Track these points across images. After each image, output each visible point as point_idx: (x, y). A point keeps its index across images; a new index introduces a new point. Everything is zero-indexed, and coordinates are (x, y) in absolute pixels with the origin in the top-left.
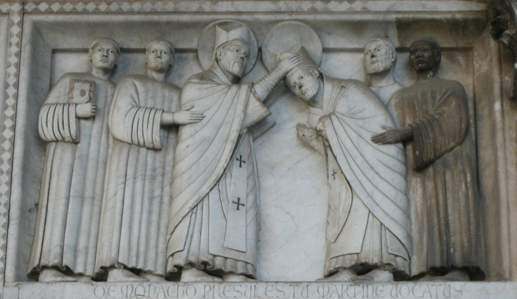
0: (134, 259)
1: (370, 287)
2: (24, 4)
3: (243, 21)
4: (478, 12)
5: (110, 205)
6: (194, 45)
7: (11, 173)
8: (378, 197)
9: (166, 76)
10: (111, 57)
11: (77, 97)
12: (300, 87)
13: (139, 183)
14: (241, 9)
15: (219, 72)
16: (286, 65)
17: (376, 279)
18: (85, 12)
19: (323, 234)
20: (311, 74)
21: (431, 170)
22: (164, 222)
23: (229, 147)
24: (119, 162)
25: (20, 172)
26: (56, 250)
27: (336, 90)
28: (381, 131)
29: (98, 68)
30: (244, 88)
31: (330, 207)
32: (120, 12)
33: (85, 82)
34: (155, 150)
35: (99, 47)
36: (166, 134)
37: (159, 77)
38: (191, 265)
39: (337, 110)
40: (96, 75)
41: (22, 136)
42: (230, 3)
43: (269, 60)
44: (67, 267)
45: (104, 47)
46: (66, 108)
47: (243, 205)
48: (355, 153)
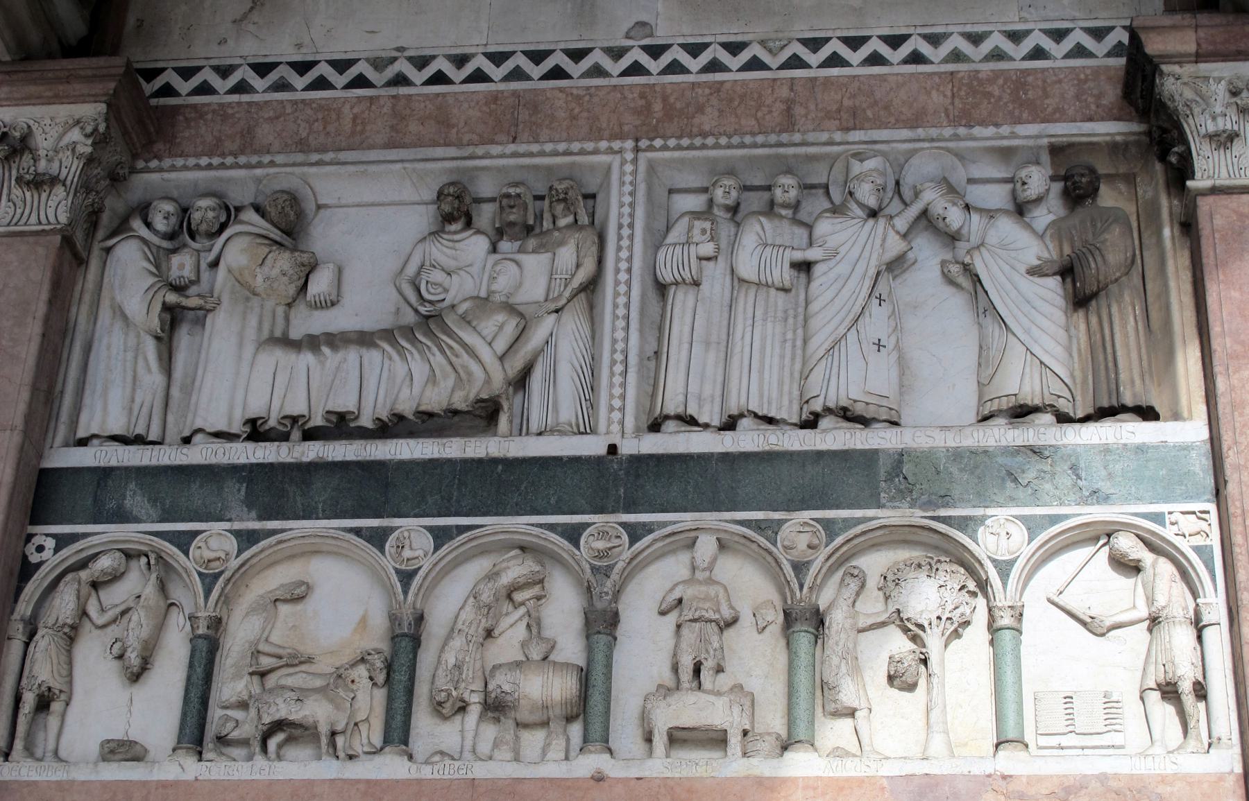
0: (765, 406)
1: (1031, 430)
2: (637, 140)
4: (1140, 133)
5: (737, 349)
7: (627, 317)
8: (1036, 332)
9: (794, 213)
10: (734, 194)
11: (697, 236)
12: (944, 219)
13: (769, 325)
15: (854, 206)
17: (1037, 422)
18: (704, 147)
19: (975, 377)
20: (955, 204)
21: (1094, 303)
22: (798, 366)
23: (868, 283)
24: (745, 303)
27: (985, 220)
28: (1037, 262)
30: (882, 222)
31: (981, 347)
32: (742, 146)
33: (706, 219)
34: (786, 290)
35: (720, 183)
36: (796, 274)
38: (828, 411)
39: (986, 241)
40: (718, 213)
41: (639, 279)
42: (862, 132)
43: (907, 193)
44: (692, 417)
45: (726, 182)
46: (686, 248)
47: (885, 347)
48: (1009, 286)
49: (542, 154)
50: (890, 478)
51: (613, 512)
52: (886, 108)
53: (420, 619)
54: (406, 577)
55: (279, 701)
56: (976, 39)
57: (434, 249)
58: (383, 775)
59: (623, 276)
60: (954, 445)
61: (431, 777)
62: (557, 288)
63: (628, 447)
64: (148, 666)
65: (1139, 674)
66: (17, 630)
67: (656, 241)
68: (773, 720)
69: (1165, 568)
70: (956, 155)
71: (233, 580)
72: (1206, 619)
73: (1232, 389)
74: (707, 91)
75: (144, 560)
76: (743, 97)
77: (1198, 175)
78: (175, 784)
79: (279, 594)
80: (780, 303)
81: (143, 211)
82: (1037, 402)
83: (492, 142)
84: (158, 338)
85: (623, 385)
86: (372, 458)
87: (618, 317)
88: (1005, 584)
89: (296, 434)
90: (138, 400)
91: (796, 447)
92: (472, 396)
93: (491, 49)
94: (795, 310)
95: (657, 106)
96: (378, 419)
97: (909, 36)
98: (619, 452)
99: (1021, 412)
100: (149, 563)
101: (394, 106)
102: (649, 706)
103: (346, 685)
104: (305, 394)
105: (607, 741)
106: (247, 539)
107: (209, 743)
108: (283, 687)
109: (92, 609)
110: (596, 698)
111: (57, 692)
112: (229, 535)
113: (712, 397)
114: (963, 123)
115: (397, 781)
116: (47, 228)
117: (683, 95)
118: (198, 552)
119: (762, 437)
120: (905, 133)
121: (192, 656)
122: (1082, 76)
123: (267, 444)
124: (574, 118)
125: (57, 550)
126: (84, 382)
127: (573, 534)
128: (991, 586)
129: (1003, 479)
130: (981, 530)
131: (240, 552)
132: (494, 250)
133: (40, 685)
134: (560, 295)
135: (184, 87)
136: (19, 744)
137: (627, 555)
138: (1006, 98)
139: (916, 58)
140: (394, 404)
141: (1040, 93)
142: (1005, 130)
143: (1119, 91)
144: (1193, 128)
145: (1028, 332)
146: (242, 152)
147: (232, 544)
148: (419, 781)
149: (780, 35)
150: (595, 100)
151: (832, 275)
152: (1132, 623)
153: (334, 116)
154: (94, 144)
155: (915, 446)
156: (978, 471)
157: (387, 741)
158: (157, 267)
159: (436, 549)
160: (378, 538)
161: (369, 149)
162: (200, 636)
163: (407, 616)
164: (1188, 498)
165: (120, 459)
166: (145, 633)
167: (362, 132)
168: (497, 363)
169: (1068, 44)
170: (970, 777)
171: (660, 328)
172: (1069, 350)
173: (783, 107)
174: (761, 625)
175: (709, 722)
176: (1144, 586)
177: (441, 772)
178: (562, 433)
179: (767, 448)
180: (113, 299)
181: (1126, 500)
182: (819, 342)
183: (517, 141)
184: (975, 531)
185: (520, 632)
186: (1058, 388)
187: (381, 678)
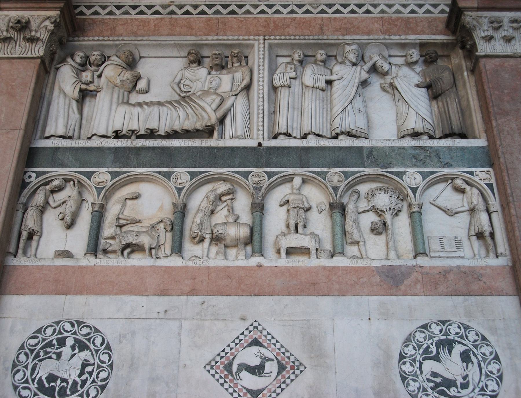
0: (318, 130)
2: (264, 36)
3: (356, 43)
4: (453, 40)
5: (306, 110)
6: (335, 54)
7: (263, 98)
13: (318, 102)
14: (355, 38)
15: (347, 62)
16: (376, 58)
18: (290, 39)
19: (395, 124)
20: (386, 62)
21: (440, 98)
22: (329, 118)
23: (355, 88)
24: (308, 94)
25: (267, 98)
26: (285, 127)
27: (397, 68)
29: (296, 60)
31: (397, 113)
33: (292, 64)
34: (323, 90)
35: (297, 52)
37: (323, 64)
38: (343, 133)
43: (366, 59)
44: (290, 134)
46: (285, 74)
48: (408, 90)
49: (228, 40)
50: (368, 157)
51: (261, 167)
52: (358, 28)
53: (185, 206)
54: (179, 190)
55: (129, 236)
56: (390, 6)
57: (186, 73)
58: (172, 264)
59: (261, 83)
60: (392, 146)
61: (192, 265)
62: (235, 87)
63: (266, 144)
64: (74, 223)
65: (467, 230)
66: (20, 208)
67: (272, 71)
68: (328, 246)
69: (475, 191)
70: (385, 45)
71: (109, 190)
72: (492, 209)
73: (498, 125)
74: (290, 20)
75: (72, 183)
76: (304, 23)
77: (479, 51)
78: (86, 267)
79: (127, 197)
80: (321, 95)
81: (72, 56)
82: (422, 131)
83: (208, 35)
84: (77, 101)
85: (263, 122)
86: (165, 146)
87: (260, 98)
88: (415, 196)
89: (133, 137)
90: (70, 123)
91: (331, 145)
92: (204, 125)
93: (207, 3)
94: (327, 98)
95: (272, 25)
96: (166, 132)
97: (365, 4)
98: (262, 145)
99: (416, 135)
100: (74, 184)
101: (170, 22)
102: (278, 239)
103: (156, 231)
104: (137, 122)
105: (262, 253)
106: (114, 175)
107: (100, 252)
108: (130, 231)
109: (51, 201)
110: (256, 236)
111: (36, 232)
112: (107, 173)
113: (297, 127)
114: (387, 34)
115: (178, 267)
116: (35, 56)
117: (281, 21)
118: (95, 180)
119: (318, 141)
120: (366, 37)
121: (92, 218)
122: (430, 20)
123: (122, 140)
124: (240, 28)
125: (37, 178)
126: (48, 117)
127: (246, 175)
128: (409, 196)
129: (411, 158)
130: (404, 176)
131: (111, 180)
132: (209, 73)
133: (29, 229)
134: (237, 90)
135: (88, 12)
136: (20, 251)
137: (267, 183)
138: (402, 26)
139: (368, 12)
140: (173, 126)
141: (415, 25)
142: (403, 37)
143: (444, 26)
144: (476, 35)
145: (417, 107)
146: (111, 36)
147: (109, 177)
148: (187, 267)
149: (317, 2)
150: (248, 22)
151: (341, 85)
152: (463, 212)
153: (147, 24)
154: (54, 26)
155: (376, 145)
156: (402, 155)
157: (173, 252)
158: (77, 75)
159: (191, 180)
160: (168, 175)
161: (161, 36)
162: (96, 211)
163: (180, 202)
164: (482, 166)
165: (63, 144)
166: (73, 209)
167: (158, 30)
168: (213, 112)
169: (424, 9)
170: (407, 267)
171: (274, 102)
172: (431, 113)
173: (319, 27)
174: (320, 210)
175: (303, 245)
176: (467, 198)
177: (196, 263)
178: (239, 138)
179: (320, 145)
180: (60, 86)
181: (459, 167)
182: (337, 109)
183: (218, 35)
184: (402, 177)
185: (225, 212)
186: (429, 127)
187: (169, 228)
